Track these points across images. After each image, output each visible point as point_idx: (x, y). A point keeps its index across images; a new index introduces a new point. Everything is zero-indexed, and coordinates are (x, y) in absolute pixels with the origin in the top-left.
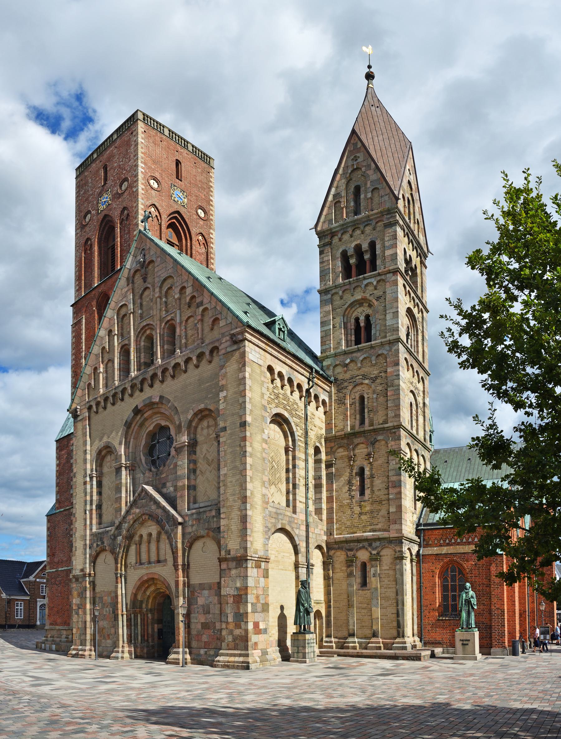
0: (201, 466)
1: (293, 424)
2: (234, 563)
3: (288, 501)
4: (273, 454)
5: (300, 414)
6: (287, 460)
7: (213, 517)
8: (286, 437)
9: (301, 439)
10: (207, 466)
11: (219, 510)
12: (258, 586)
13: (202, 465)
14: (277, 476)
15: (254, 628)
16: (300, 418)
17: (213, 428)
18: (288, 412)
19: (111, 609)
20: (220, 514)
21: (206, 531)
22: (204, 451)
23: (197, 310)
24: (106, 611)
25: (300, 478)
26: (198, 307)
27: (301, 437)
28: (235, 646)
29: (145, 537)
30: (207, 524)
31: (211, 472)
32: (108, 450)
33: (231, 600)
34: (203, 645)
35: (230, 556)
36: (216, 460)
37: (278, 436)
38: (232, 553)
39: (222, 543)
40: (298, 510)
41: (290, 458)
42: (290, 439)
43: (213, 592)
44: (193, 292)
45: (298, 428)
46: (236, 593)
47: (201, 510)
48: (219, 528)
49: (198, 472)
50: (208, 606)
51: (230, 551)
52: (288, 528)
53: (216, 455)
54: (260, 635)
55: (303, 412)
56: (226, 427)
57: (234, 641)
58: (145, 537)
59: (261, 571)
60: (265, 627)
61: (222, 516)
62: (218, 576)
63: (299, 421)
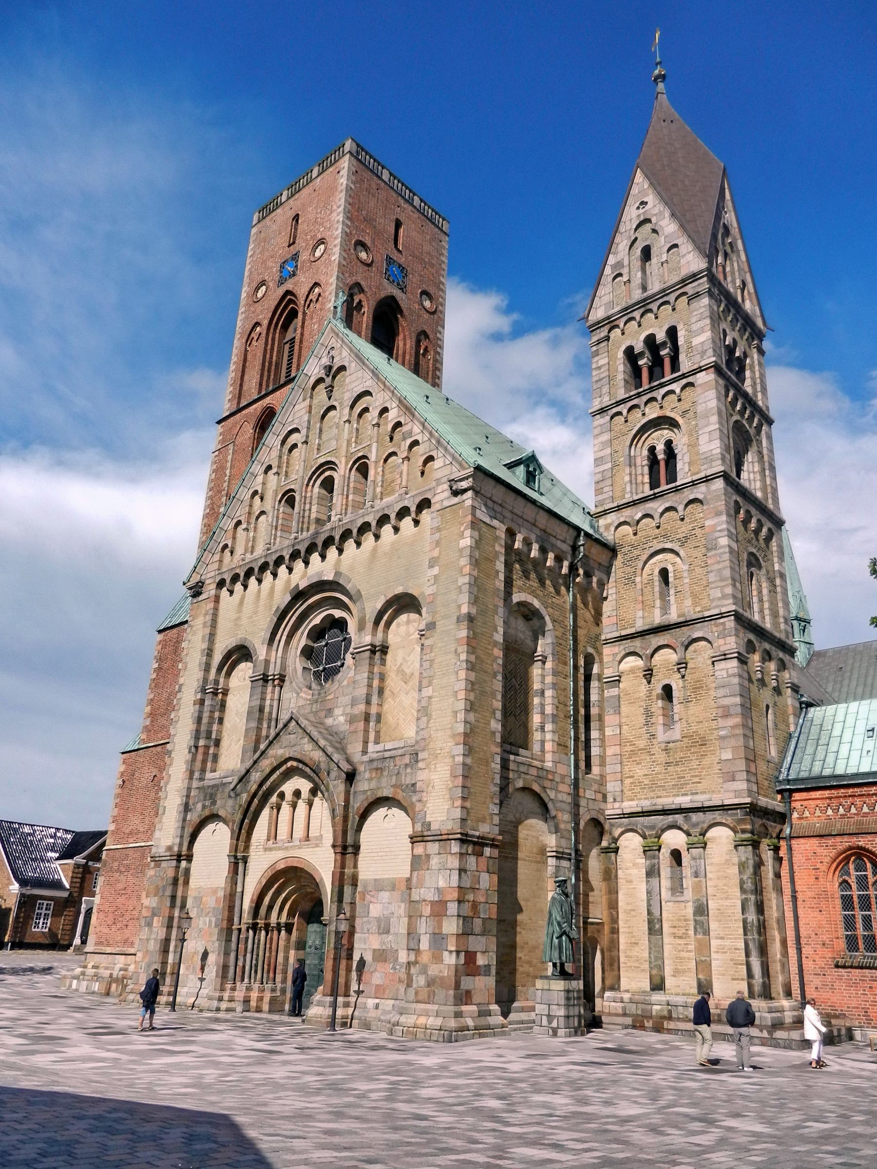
0: (392, 684)
2: (437, 844)
7: (406, 765)
10: (403, 683)
11: (417, 754)
12: (477, 887)
13: (393, 682)
15: (466, 963)
17: (416, 624)
18: (540, 600)
19: (214, 919)
20: (417, 761)
21: (392, 790)
22: (400, 660)
23: (403, 443)
24: (205, 923)
26: (404, 439)
28: (429, 997)
29: (289, 796)
30: (394, 778)
31: (407, 694)
32: (244, 651)
33: (427, 910)
34: (373, 992)
35: (429, 833)
36: (417, 675)
38: (434, 827)
39: (417, 809)
43: (397, 894)
44: (399, 416)
46: (436, 899)
47: (387, 754)
48: (414, 785)
49: (387, 693)
50: (387, 920)
51: (429, 824)
52: (536, 787)
53: (418, 666)
54: (477, 978)
56: (435, 623)
57: (429, 985)
58: (289, 796)
59: (483, 861)
60: (486, 963)
61: (421, 765)
62: (408, 868)
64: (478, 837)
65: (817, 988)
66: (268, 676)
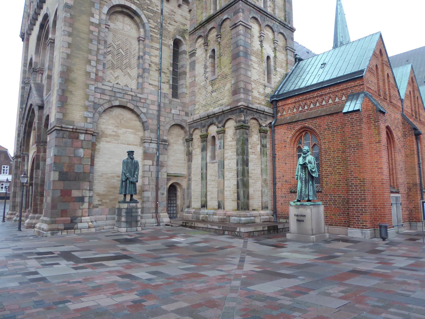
1: (143, 17)
3: (138, 83)
4: (119, 42)
5: (155, 9)
6: (139, 48)
8: (139, 28)
9: (154, 30)
14: (125, 62)
16: (154, 12)
25: (151, 64)
27: (155, 29)
37: (129, 28)
40: (146, 91)
41: (141, 46)
42: (142, 30)
45: (150, 20)
55: (159, 8)
63: (152, 15)
64: (73, 129)
65: (282, 204)
66: (36, 69)
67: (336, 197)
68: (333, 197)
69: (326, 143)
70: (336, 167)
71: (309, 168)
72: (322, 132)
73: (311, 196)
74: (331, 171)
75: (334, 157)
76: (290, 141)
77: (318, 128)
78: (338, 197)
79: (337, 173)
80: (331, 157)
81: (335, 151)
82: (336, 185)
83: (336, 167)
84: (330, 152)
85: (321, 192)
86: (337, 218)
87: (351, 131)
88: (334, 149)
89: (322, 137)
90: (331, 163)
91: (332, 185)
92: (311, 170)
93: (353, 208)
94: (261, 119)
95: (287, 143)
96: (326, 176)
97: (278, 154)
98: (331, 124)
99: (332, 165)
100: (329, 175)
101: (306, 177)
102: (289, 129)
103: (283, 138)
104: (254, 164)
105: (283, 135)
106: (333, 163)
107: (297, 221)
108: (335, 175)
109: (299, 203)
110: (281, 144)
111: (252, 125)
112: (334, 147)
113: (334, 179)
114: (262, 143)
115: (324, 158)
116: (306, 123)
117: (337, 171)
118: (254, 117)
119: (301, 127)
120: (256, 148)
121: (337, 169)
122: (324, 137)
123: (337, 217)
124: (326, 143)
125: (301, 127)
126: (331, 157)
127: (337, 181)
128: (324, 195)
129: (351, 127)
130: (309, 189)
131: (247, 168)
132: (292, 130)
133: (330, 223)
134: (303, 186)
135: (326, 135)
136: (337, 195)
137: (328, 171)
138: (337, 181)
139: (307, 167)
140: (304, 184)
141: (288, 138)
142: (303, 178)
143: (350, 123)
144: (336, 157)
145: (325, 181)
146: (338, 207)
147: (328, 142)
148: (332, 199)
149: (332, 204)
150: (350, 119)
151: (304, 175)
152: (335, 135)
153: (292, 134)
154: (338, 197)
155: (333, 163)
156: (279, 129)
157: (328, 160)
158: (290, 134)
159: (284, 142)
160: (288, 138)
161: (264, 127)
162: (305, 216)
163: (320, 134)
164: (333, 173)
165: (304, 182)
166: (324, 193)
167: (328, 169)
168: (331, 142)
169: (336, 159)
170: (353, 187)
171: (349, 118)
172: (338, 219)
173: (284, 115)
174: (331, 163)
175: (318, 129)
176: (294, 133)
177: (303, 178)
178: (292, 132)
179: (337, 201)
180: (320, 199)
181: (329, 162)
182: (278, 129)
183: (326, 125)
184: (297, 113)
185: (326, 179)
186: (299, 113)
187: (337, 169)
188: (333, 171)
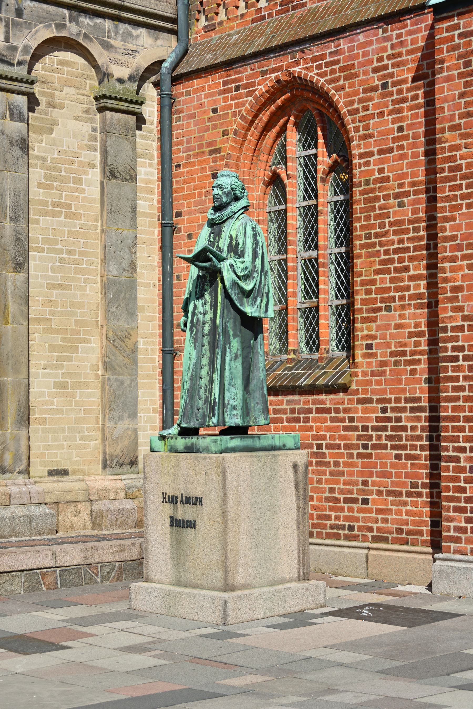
67: (403, 410)
68: (393, 410)
69: (371, 154)
70: (407, 269)
71: (228, 276)
72: (360, 101)
73: (234, 408)
74: (387, 290)
75: (401, 222)
76: (232, 148)
77: (341, 82)
78: (413, 410)
79: (411, 297)
80: (391, 224)
81: (407, 194)
82: (403, 354)
83: (407, 269)
84: (386, 197)
85: (345, 389)
86: (403, 508)
87: (462, 96)
88: (400, 186)
89: (357, 129)
90: (387, 252)
91: (392, 354)
92: (234, 284)
93: (457, 460)
94: (107, 46)
95: (222, 158)
96: (368, 311)
97: (189, 213)
98: (393, 66)
99: (391, 261)
100: (379, 310)
101: (214, 320)
102: (228, 91)
103: (208, 137)
104: (62, 260)
105: (210, 120)
106: (396, 251)
107: (171, 525)
108: (403, 307)
109: (181, 442)
110: (200, 163)
111: (57, 71)
112: (404, 176)
113: (398, 326)
114: (109, 162)
115: (362, 227)
116: (297, 63)
117: (408, 288)
118: (64, 34)
119: (278, 81)
120: (78, 181)
121: (411, 278)
122: (366, 128)
123: (405, 504)
124: (371, 154)
125: (278, 81)
126: (391, 224)
127: (411, 335)
128: (360, 401)
129: (461, 76)
130: (227, 373)
131: (21, 276)
132: (240, 97)
133: (379, 529)
134: (205, 361)
135: (372, 116)
136: (407, 400)
137: (379, 291)
138: (411, 335)
139: (220, 271)
140: (208, 354)
141: (225, 133)
142: (204, 323)
143: (460, 57)
144: (410, 222)
145: (363, 338)
146: (408, 457)
147: (380, 152)
148: (389, 419)
149: (389, 443)
150: (461, 36)
151: (208, 307)
152: (406, 118)
153: (243, 118)
154: (413, 410)
155: (396, 251)
156: (196, 91)
157: (377, 235)
158: (234, 114)
159: (211, 153)
160: (225, 133)
161: (121, 81)
162: (199, 501)
163: (350, 113)
164: (393, 299)
165: (206, 340)
166: (356, 392)
167: (373, 282)
168: (391, 150)
169: (407, 231)
170: (461, 363)
171: (457, 33)
172: (408, 513)
173: (221, 23)
174: (387, 252)
175: (343, 88)
176: (248, 112)
177: (204, 323)
178: (243, 105)
179: (404, 429)
180: (343, 420)
181: (381, 245)
182: (188, 93)
183: (375, 70)
184: (270, 15)
185: (369, 329)
186: (278, 13)
187: (411, 278)
188: (397, 289)
